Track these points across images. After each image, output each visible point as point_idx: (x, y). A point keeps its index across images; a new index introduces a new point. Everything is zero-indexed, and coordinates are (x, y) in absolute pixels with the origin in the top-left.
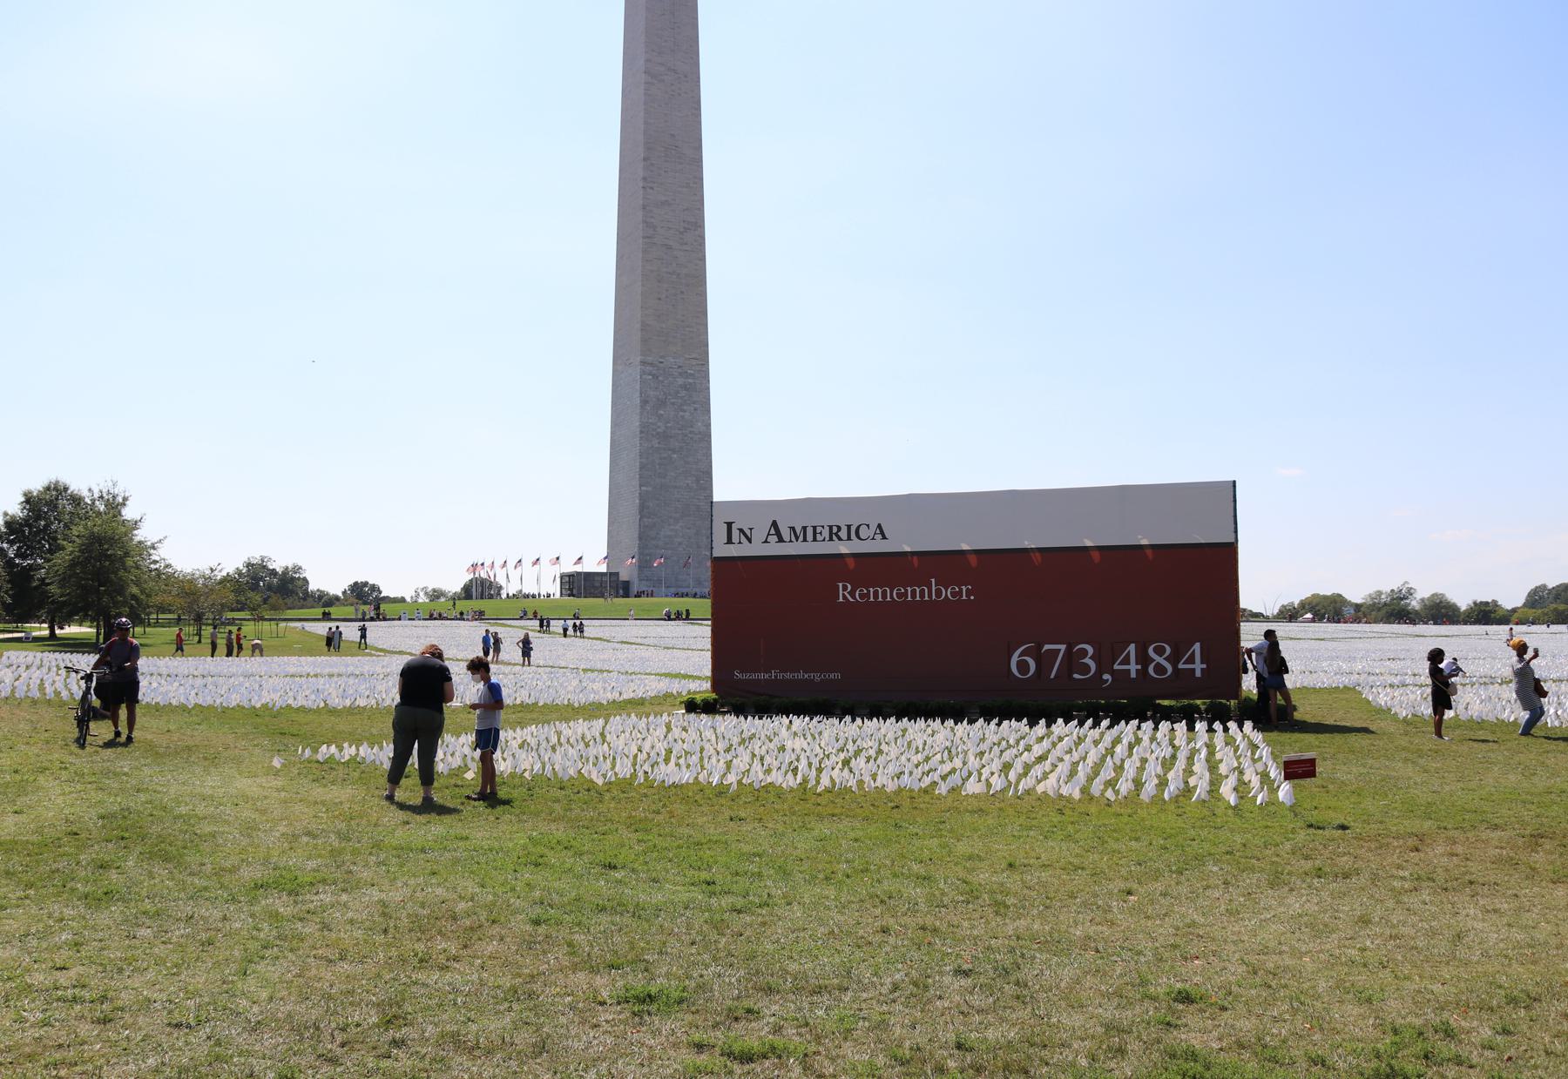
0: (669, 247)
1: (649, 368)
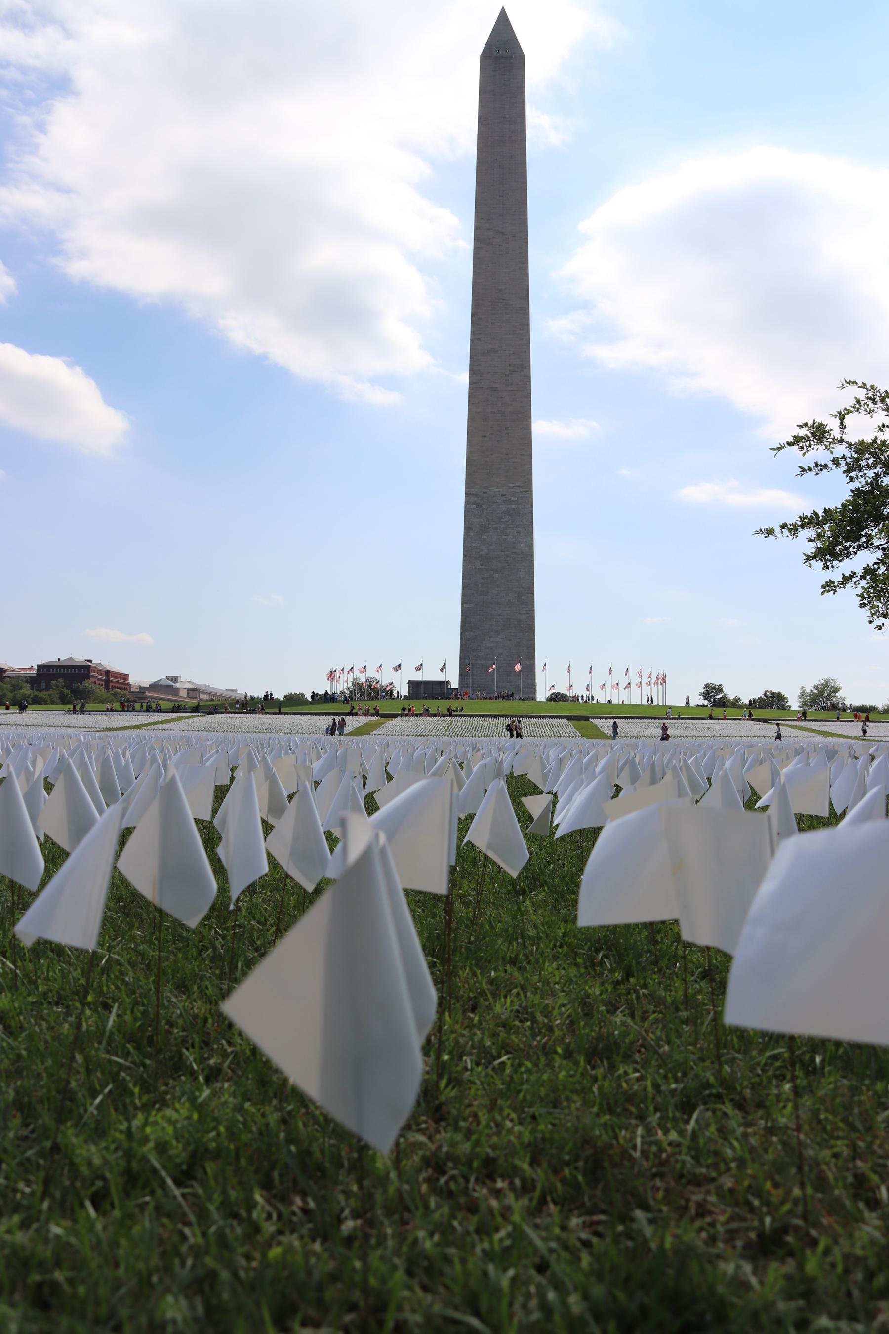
0: (496, 390)
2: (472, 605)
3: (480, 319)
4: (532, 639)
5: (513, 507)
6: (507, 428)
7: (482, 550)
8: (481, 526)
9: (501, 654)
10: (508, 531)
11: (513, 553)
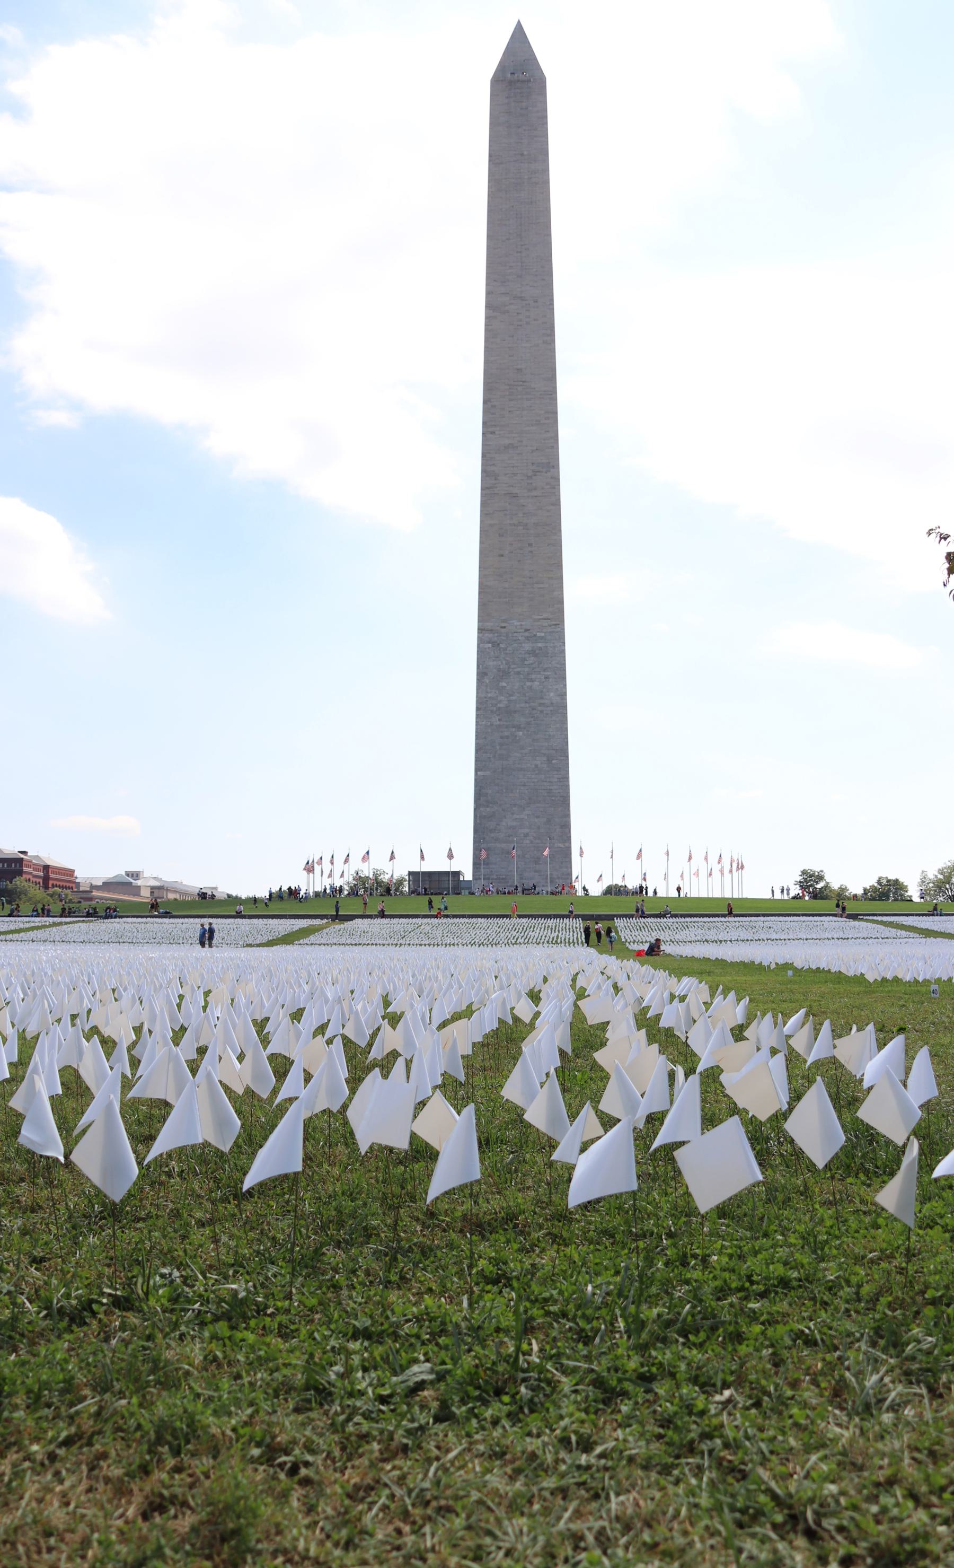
0: (515, 496)
2: (488, 773)
3: (493, 406)
4: (567, 815)
6: (530, 545)
7: (500, 702)
8: (499, 670)
9: (526, 835)
10: (533, 676)
11: (541, 705)
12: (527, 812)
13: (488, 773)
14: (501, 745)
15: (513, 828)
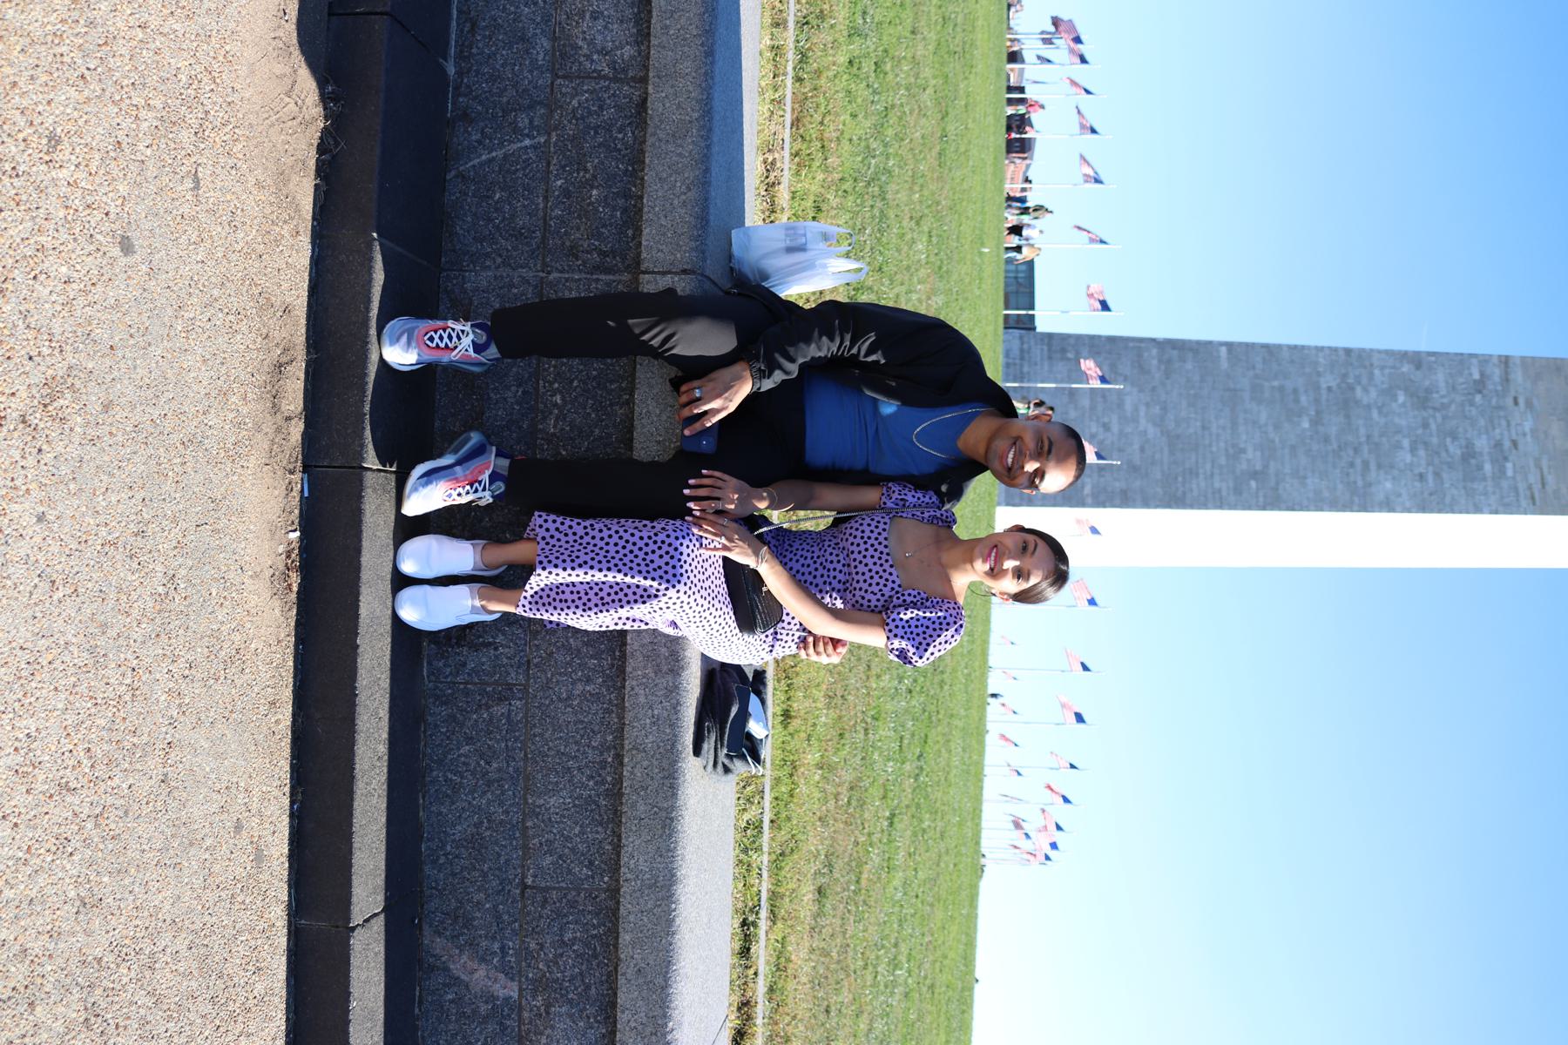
1: (1496, 374)
2: (1224, 365)
5: (1488, 467)
7: (1366, 390)
9: (1106, 427)
11: (1366, 464)
12: (1152, 431)
13: (1224, 365)
14: (1281, 389)
15: (1120, 405)
